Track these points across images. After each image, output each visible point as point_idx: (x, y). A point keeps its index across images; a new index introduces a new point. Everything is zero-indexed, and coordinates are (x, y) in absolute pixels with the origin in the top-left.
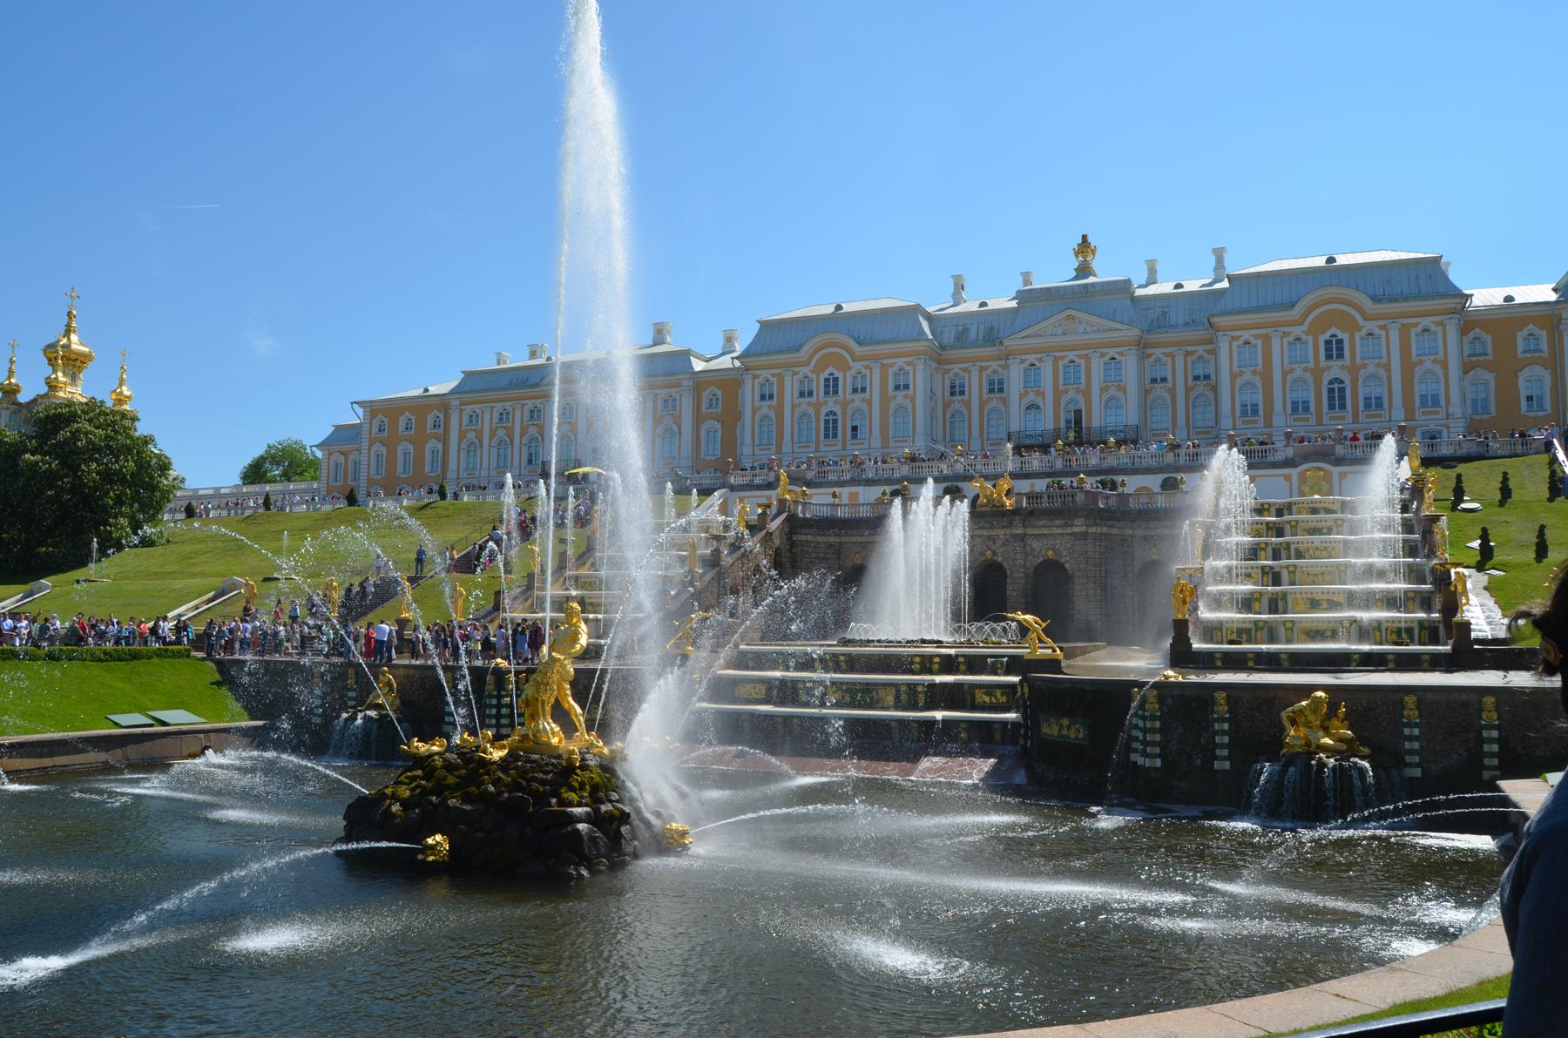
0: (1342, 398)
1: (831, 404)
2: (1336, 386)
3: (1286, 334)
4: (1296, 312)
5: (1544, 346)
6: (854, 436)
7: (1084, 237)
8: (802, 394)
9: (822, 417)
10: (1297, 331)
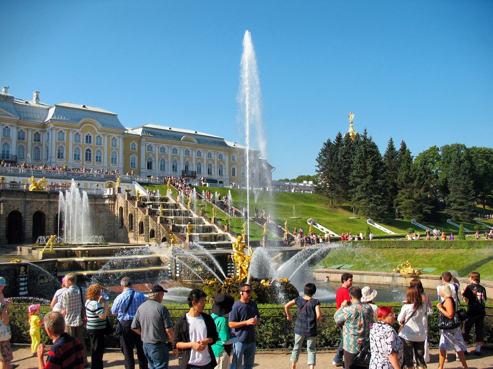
0: (90, 157)
2: (88, 152)
3: (75, 131)
4: (80, 123)
5: (137, 147)
10: (78, 131)
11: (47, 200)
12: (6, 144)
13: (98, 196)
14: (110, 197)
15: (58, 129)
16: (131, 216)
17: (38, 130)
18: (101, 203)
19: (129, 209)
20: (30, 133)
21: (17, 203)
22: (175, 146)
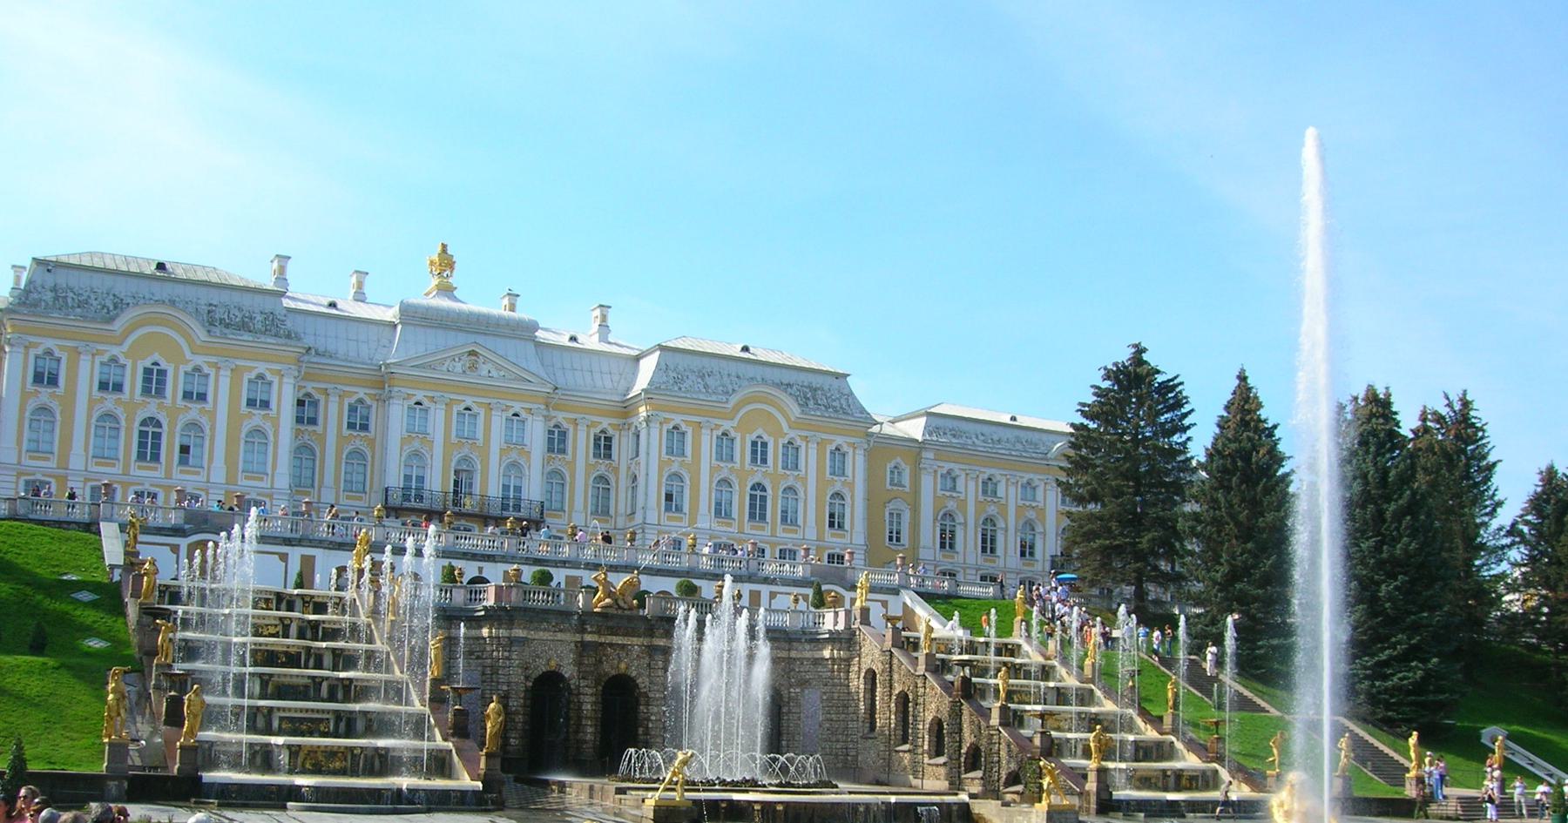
0: (763, 508)
1: (152, 408)
2: (758, 493)
5: (906, 480)
6: (184, 461)
7: (444, 246)
8: (103, 386)
9: (137, 424)
11: (646, 641)
12: (514, 465)
13: (796, 632)
14: (834, 638)
15: (667, 421)
16: (903, 700)
17: (605, 423)
18: (808, 655)
19: (896, 677)
20: (582, 435)
21: (557, 651)
22: (1027, 476)
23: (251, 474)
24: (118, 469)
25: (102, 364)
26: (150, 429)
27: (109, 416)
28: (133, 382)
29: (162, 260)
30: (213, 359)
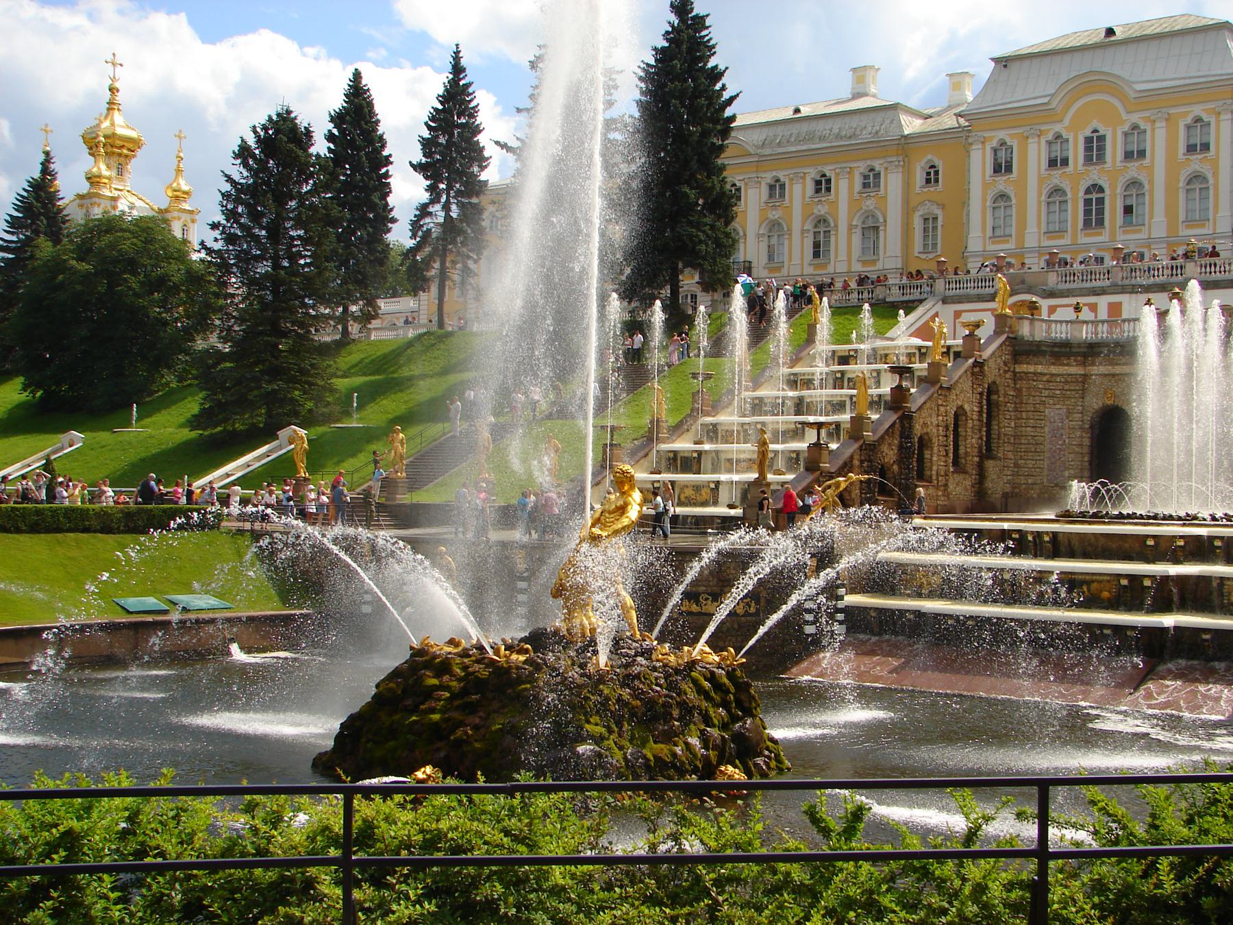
1: (1095, 175)
6: (1127, 223)
8: (1052, 163)
9: (1081, 194)
23: (1190, 222)
24: (1066, 241)
25: (1049, 143)
26: (1094, 196)
27: (1057, 191)
28: (1076, 153)
29: (1108, 26)
30: (1147, 114)
